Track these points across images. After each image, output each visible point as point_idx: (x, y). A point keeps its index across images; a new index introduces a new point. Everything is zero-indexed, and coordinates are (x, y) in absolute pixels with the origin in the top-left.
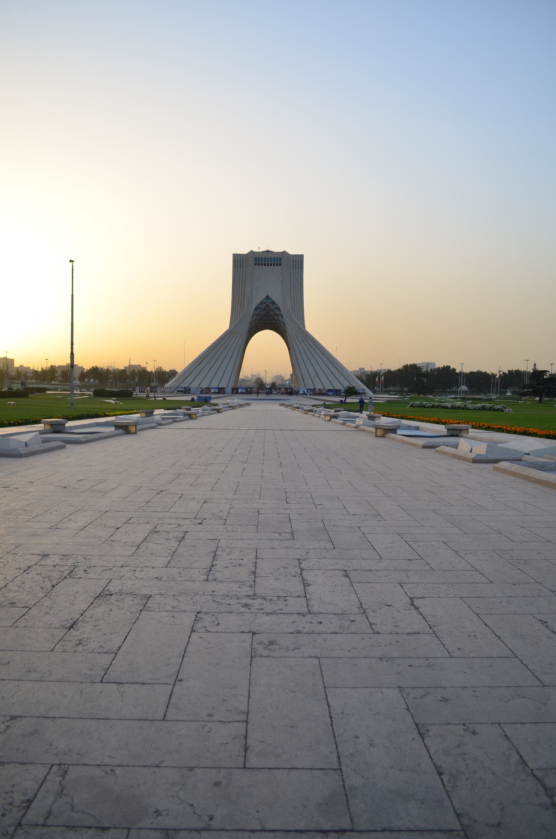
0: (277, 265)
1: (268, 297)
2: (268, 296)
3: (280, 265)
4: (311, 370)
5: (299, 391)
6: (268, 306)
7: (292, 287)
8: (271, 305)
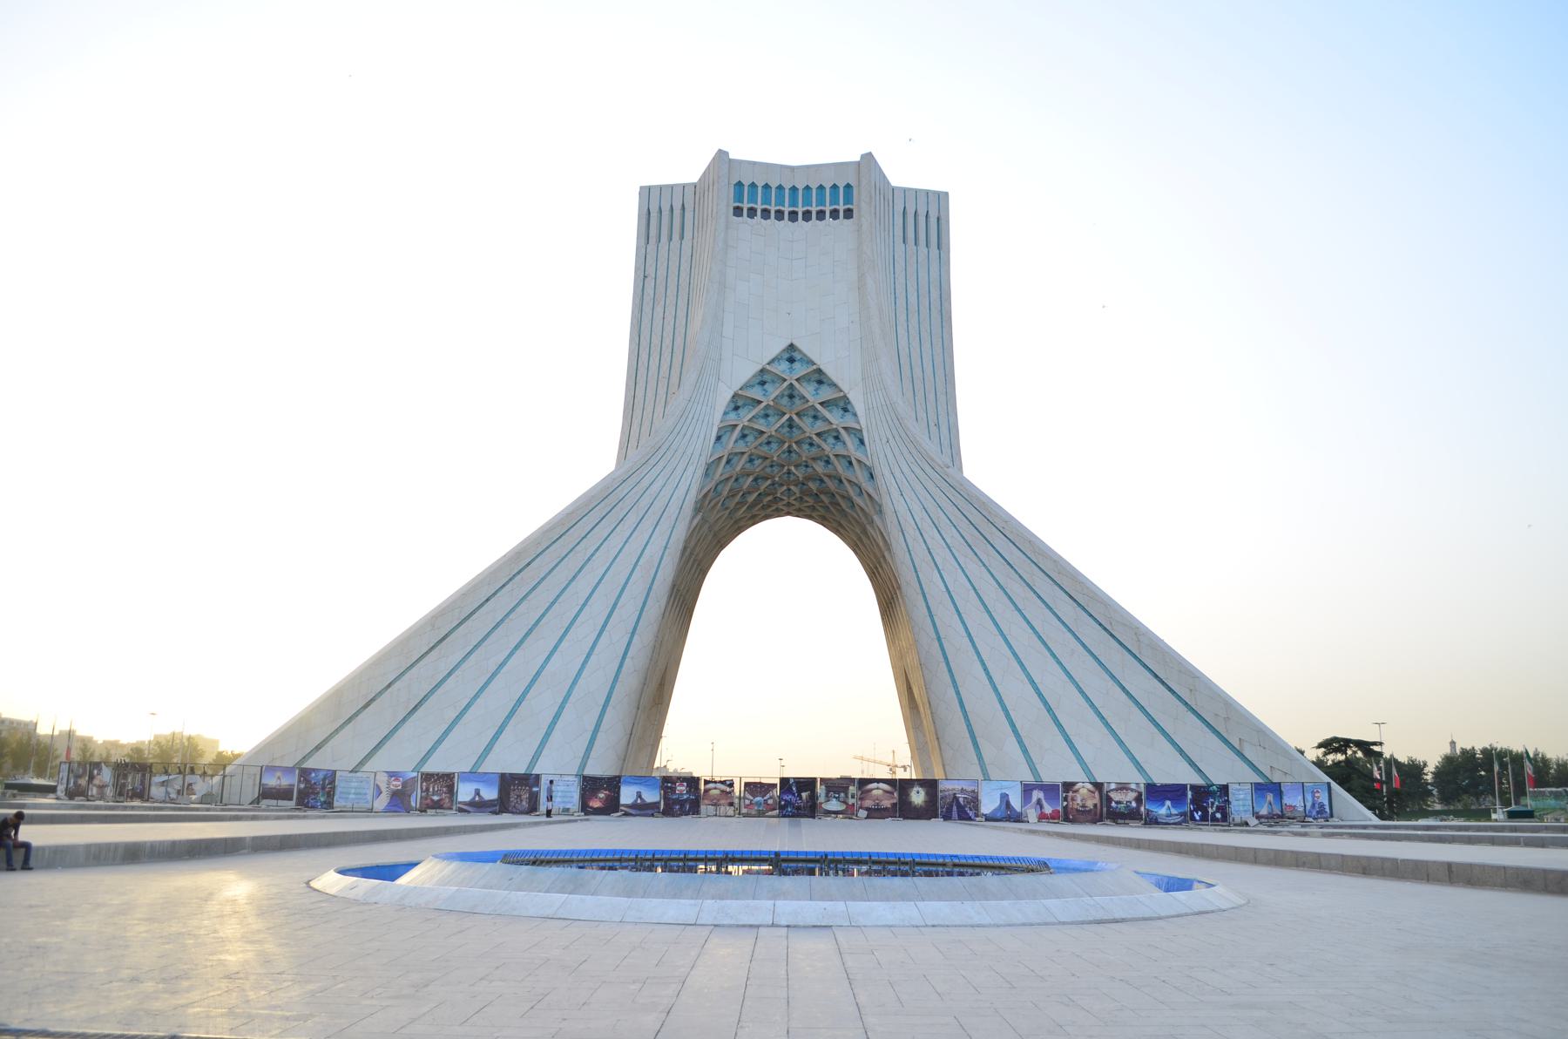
0: (835, 214)
1: (791, 354)
2: (792, 347)
3: (849, 214)
4: (1015, 689)
5: (974, 801)
7: (902, 318)
8: (807, 390)
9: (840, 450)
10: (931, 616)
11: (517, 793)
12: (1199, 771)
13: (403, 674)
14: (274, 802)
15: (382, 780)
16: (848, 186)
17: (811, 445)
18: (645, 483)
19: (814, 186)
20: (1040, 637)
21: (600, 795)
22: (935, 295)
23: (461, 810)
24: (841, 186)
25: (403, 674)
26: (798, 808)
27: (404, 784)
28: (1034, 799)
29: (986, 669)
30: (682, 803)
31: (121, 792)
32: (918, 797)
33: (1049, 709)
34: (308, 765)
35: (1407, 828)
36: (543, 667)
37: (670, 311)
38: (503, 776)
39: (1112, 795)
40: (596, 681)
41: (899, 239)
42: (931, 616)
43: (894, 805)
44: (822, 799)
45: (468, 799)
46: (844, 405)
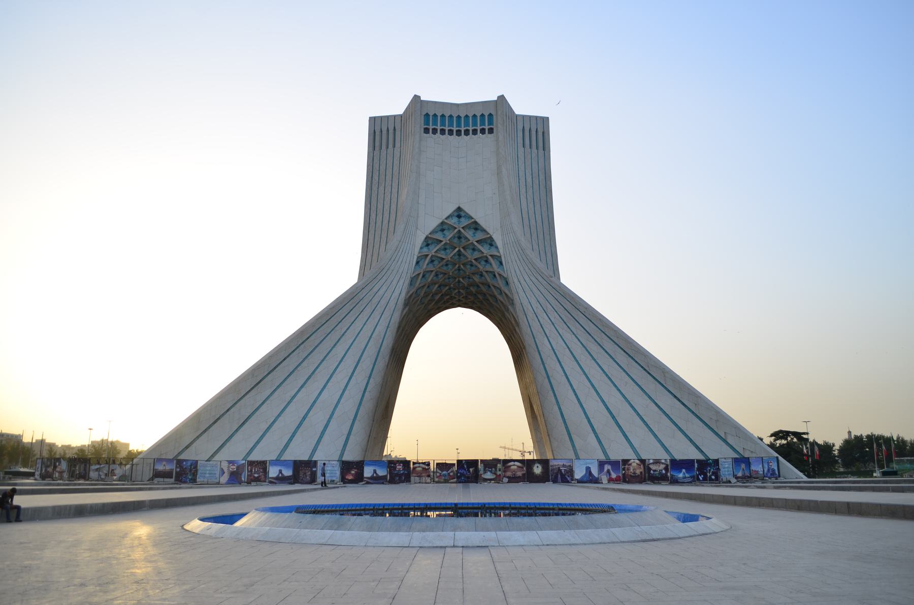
0: (483, 131)
1: (459, 213)
2: (459, 209)
3: (491, 131)
5: (571, 471)
6: (460, 236)
7: (523, 191)
8: (469, 234)
9: (488, 268)
10: (543, 364)
11: (304, 472)
12: (701, 452)
13: (235, 404)
14: (162, 479)
15: (225, 465)
16: (490, 115)
17: (472, 265)
18: (375, 289)
19: (470, 115)
20: (607, 375)
21: (352, 472)
22: (542, 177)
23: (271, 482)
24: (486, 115)
25: (235, 404)
26: (468, 478)
27: (238, 468)
28: (606, 470)
29: (576, 394)
30: (400, 476)
31: (73, 476)
32: (538, 470)
33: (613, 417)
34: (181, 457)
35: (823, 482)
36: (317, 398)
37: (388, 189)
38: (295, 462)
39: (651, 466)
40: (348, 406)
41: (520, 145)
42: (543, 364)
43: (524, 475)
44: (481, 472)
45: (275, 475)
46: (490, 242)
